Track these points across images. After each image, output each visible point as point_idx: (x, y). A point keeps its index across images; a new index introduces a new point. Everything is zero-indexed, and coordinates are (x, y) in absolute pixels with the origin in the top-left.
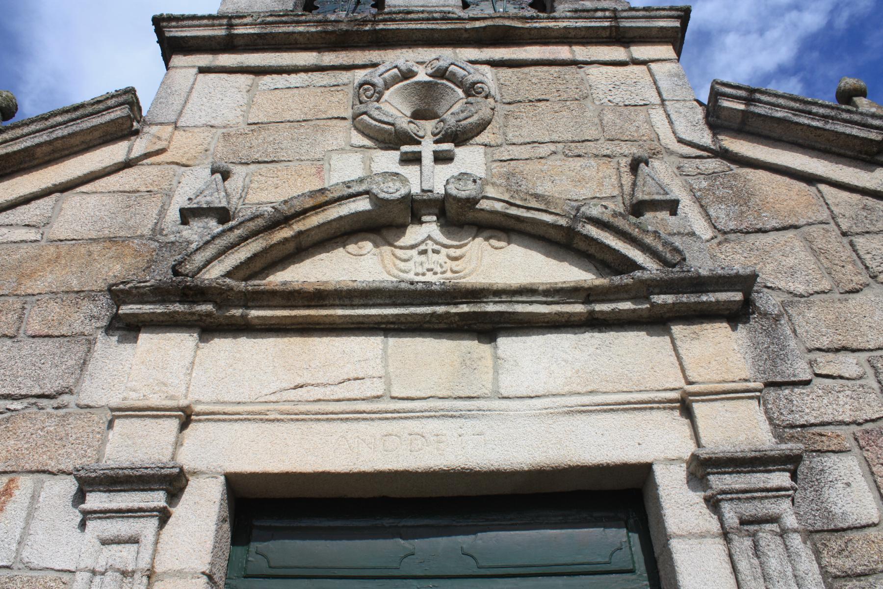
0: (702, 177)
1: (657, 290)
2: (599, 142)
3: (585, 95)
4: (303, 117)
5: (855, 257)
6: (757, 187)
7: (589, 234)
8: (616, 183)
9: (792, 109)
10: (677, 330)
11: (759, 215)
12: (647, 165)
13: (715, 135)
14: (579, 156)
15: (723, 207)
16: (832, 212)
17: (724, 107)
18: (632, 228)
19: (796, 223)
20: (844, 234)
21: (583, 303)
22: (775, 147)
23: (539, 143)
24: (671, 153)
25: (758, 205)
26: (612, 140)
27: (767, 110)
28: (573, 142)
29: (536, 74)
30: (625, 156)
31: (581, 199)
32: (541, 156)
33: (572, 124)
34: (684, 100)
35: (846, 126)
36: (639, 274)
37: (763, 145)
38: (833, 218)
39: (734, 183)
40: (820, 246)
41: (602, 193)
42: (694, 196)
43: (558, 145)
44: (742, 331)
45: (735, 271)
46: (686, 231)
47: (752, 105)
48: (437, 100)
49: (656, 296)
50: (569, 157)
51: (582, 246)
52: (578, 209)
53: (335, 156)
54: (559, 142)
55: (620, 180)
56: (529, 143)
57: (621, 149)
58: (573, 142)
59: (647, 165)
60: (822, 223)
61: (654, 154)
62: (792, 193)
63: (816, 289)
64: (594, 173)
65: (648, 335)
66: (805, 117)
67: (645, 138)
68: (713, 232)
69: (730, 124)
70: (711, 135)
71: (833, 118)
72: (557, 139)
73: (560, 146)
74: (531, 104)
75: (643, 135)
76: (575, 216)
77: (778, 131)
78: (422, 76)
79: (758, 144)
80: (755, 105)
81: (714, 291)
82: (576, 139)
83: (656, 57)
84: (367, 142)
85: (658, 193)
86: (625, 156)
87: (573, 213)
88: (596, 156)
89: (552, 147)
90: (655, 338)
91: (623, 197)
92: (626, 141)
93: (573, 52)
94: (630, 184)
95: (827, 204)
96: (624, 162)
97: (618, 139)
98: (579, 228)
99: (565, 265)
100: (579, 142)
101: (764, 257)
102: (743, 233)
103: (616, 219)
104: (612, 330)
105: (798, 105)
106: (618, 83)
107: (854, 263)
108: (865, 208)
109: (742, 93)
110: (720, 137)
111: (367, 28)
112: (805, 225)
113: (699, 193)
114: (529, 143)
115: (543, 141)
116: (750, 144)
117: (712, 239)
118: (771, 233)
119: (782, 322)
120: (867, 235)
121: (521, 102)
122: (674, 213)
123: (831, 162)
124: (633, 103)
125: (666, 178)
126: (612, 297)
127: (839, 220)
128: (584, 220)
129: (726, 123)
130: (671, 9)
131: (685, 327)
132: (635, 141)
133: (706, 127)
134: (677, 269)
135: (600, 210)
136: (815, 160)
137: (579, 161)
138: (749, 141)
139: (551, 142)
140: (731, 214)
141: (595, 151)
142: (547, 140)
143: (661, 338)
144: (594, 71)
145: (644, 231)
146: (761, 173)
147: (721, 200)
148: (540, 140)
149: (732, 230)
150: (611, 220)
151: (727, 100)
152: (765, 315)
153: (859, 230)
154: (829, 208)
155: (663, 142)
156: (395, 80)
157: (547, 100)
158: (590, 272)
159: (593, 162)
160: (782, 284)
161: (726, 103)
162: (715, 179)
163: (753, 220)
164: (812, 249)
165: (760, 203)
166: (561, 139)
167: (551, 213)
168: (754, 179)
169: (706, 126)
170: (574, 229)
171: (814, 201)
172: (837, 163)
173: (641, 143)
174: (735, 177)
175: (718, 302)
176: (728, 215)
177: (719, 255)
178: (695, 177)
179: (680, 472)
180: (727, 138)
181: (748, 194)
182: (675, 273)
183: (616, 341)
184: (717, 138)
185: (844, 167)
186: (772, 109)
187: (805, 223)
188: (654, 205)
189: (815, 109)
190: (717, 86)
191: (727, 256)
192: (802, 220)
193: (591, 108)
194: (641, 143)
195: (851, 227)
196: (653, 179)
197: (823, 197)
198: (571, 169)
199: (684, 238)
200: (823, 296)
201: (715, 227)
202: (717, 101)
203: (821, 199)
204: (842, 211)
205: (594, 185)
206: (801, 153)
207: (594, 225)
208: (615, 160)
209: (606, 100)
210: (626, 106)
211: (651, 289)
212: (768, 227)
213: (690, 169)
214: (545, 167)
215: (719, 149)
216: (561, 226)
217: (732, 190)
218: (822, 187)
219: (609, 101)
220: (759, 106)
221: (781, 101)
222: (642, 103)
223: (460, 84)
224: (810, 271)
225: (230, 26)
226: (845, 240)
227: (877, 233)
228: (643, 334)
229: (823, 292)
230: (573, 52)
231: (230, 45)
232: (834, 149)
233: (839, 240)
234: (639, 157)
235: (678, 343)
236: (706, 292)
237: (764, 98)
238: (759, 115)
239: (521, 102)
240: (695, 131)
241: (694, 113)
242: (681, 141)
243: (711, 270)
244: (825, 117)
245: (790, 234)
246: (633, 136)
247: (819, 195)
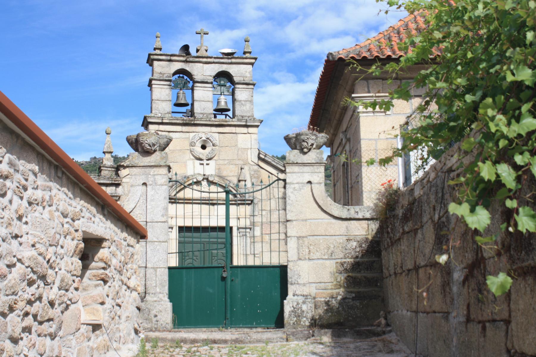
4: (180, 149)
13: (258, 160)
24: (249, 164)
44: (250, 206)
48: (207, 143)
53: (188, 161)
72: (229, 159)
78: (204, 138)
84: (193, 158)
93: (236, 130)
111: (193, 122)
130: (259, 120)
142: (227, 159)
144: (239, 136)
147: (255, 177)
156: (199, 140)
159: (234, 166)
161: (261, 156)
174: (259, 171)
179: (236, 228)
182: (241, 199)
188: (242, 180)
223: (212, 142)
225: (162, 119)
230: (236, 130)
231: (162, 123)
244: (277, 163)
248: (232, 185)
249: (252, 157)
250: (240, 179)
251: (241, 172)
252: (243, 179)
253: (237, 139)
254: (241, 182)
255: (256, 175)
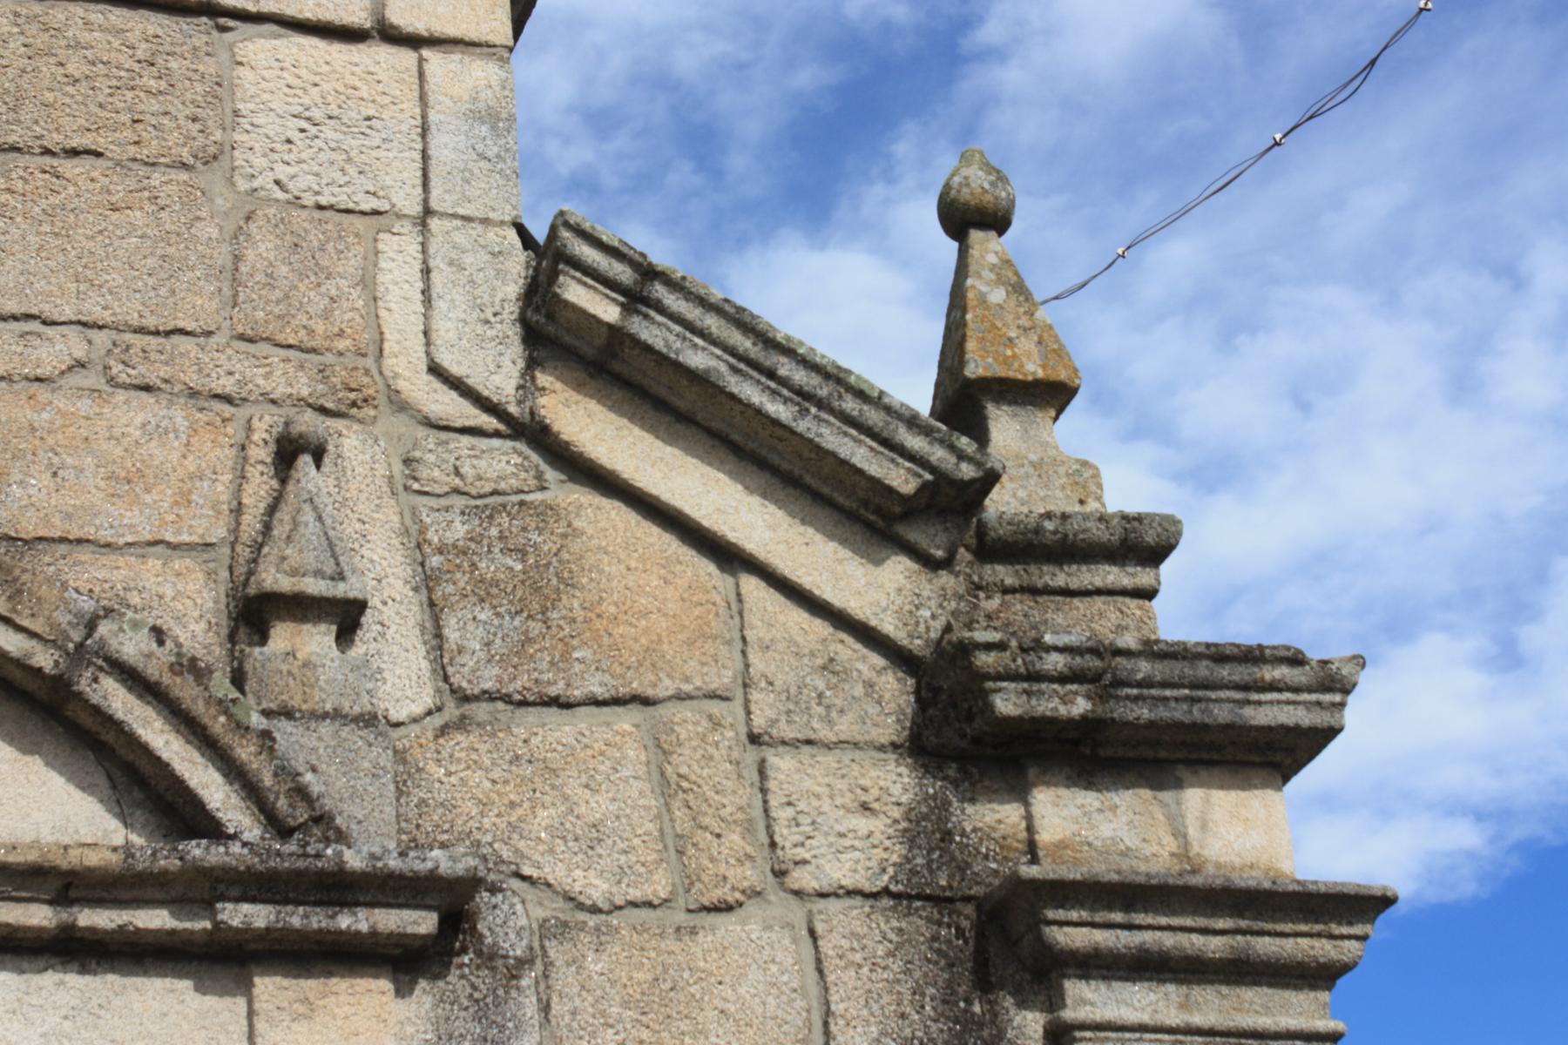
0: (459, 502)
1: (234, 892)
2: (213, 340)
3: (212, 150)
5: (757, 812)
6: (590, 559)
7: (104, 704)
8: (224, 498)
9: (731, 351)
10: (267, 986)
11: (566, 656)
12: (318, 464)
13: (532, 364)
14: (147, 388)
15: (483, 617)
16: (747, 666)
17: (567, 304)
18: (213, 711)
19: (650, 692)
20: (754, 739)
21: (51, 903)
22: (670, 439)
23: (45, 323)
24: (400, 405)
25: (574, 620)
26: (251, 340)
27: (672, 338)
28: (141, 330)
29: (85, 37)
30: (273, 402)
31: (121, 541)
32: (39, 372)
33: (150, 262)
34: (485, 221)
35: (846, 434)
36: (197, 852)
37: (642, 427)
38: (745, 686)
39: (534, 537)
40: (684, 770)
41: (178, 532)
42: (422, 564)
43: (94, 334)
44: (424, 995)
45: (429, 865)
46: (357, 709)
47: (638, 312)
49: (229, 906)
50: (118, 386)
51: (86, 720)
52: (91, 626)
54: (100, 327)
55: (239, 489)
56: (15, 318)
57: (267, 376)
58: (141, 330)
59: (318, 464)
60: (713, 696)
61: (354, 404)
62: (670, 593)
63: (635, 894)
64: (175, 456)
65: (197, 989)
66: (758, 382)
67: (342, 344)
68: (438, 691)
69: (577, 343)
70: (521, 364)
71: (821, 404)
72: (94, 311)
73: (102, 338)
74: (48, 160)
75: (341, 334)
76: (80, 646)
77: (686, 399)
79: (631, 419)
80: (646, 316)
81: (372, 905)
82: (151, 322)
83: (451, 31)
85: (318, 573)
86: (273, 402)
87: (77, 636)
88: (194, 394)
89: (73, 345)
90: (211, 1001)
91: (233, 550)
92: (290, 347)
94: (262, 506)
95: (744, 639)
96: (266, 424)
97: (267, 339)
98: (83, 685)
99: (35, 764)
100: (157, 333)
101: (539, 786)
102: (510, 702)
103: (178, 680)
104: (113, 970)
105: (748, 344)
106: (317, 114)
107: (748, 829)
108: (828, 666)
109: (622, 272)
110: (543, 379)
112: (670, 698)
113: (435, 561)
114: (15, 318)
115: (56, 317)
116: (612, 416)
117: (429, 713)
118: (583, 710)
119: (524, 982)
120: (806, 749)
121: (18, 150)
122: (347, 631)
123: (792, 514)
124: (343, 201)
125: (363, 497)
126: (124, 895)
127: (755, 696)
128: (100, 662)
129: (568, 339)
131: (286, 982)
132: (314, 351)
133: (514, 333)
134: (292, 847)
135: (143, 646)
136: (756, 500)
137: (143, 408)
138: (611, 408)
139: (79, 323)
140: (498, 641)
141: (193, 380)
142: (68, 313)
143: (227, 1002)
145: (238, 725)
146: (616, 513)
147: (485, 591)
148: (48, 310)
149: (485, 692)
150: (167, 679)
151: (580, 281)
152: (489, 958)
153: (790, 733)
154: (744, 653)
155: (389, 362)
157: (99, 155)
158: (92, 794)
159: (179, 416)
160: (555, 872)
161: (576, 292)
162: (491, 517)
163: (545, 665)
164: (663, 774)
165: (579, 613)
166: (107, 317)
167: (20, 629)
168: (590, 531)
169: (518, 328)
170: (69, 684)
171: (716, 626)
172: (803, 522)
173: (329, 358)
175: (374, 933)
176: (488, 644)
177: (432, 767)
178: (443, 502)
180: (558, 386)
181: (561, 579)
183: (117, 1002)
184: (533, 379)
185: (818, 537)
186: (684, 339)
187: (670, 692)
188: (302, 607)
189: (785, 368)
190: (565, 234)
191: (449, 774)
192: (667, 682)
193: (220, 201)
194: (329, 358)
195: (774, 722)
196: (320, 518)
197: (741, 614)
198: (117, 432)
199: (345, 732)
200: (644, 913)
201: (446, 678)
202: (554, 275)
203: (737, 619)
204: (771, 671)
205: (161, 497)
206: (730, 474)
207: (123, 682)
208: (243, 413)
209: (264, 181)
210: (320, 207)
211: (221, 888)
212: (577, 693)
213: (436, 473)
214: (45, 415)
215: (527, 417)
216: (40, 670)
217: (523, 561)
218: (752, 586)
219: (277, 182)
220: (653, 322)
221: (712, 323)
222: (368, 204)
224: (636, 841)
226: (751, 755)
227: (829, 747)
228: (185, 985)
229: (649, 905)
232: (808, 479)
233: (735, 755)
234: (301, 436)
235: (260, 1025)
236: (351, 904)
237: (672, 301)
238: (648, 349)
239: (18, 150)
240: (481, 341)
241: (498, 272)
242: (435, 370)
243: (373, 856)
244: (804, 395)
245: (626, 720)
246: (311, 332)
247: (734, 606)
248: (132, 646)
249: (445, 329)
250: (273, 579)
251: (272, 509)
252: (314, 587)
253: (220, 91)
254: (283, 636)
255: (497, 565)
